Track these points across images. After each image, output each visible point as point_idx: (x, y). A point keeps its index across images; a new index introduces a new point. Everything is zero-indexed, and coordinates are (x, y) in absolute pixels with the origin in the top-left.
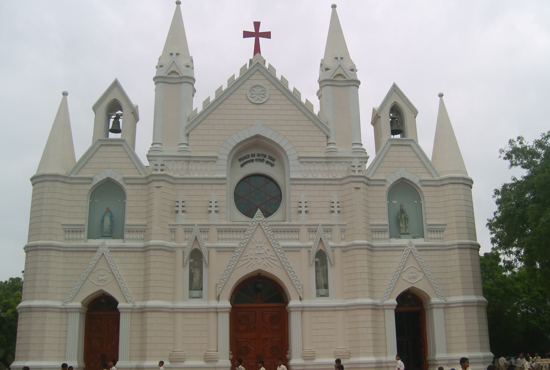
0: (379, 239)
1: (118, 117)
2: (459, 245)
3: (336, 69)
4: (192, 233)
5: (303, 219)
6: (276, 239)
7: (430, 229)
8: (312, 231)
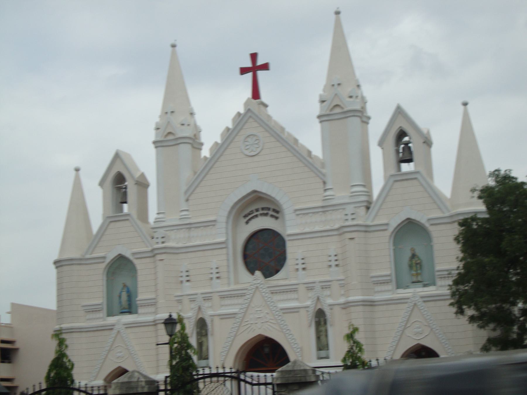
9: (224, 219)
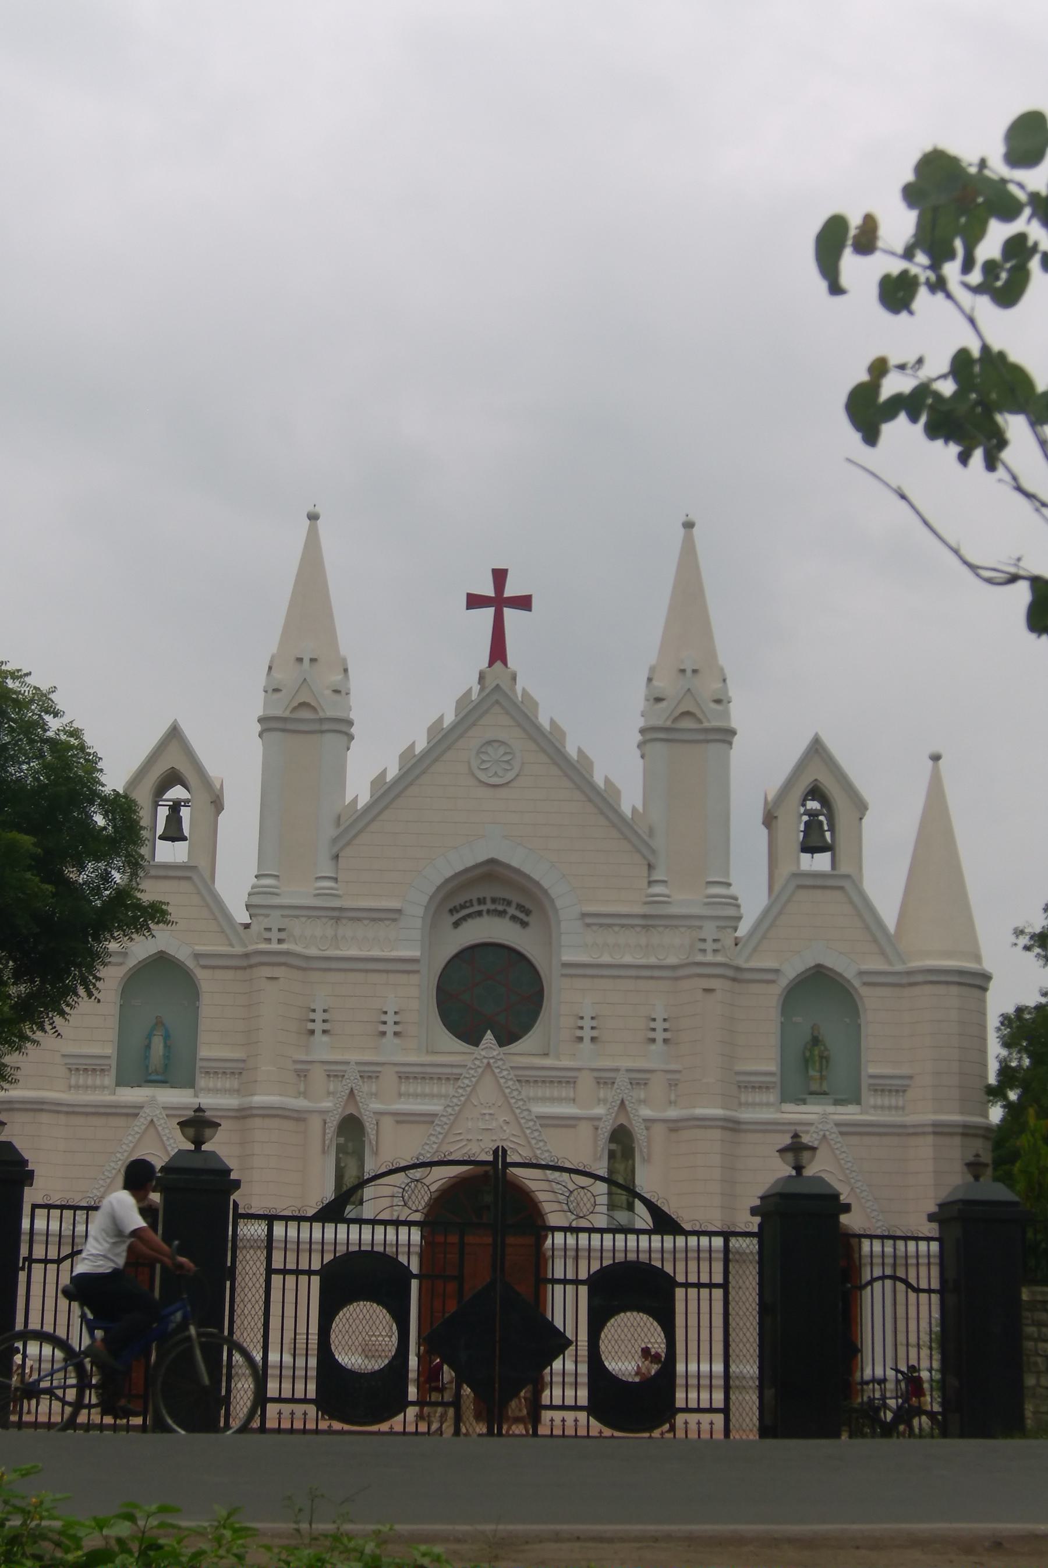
0: (754, 1105)
1: (175, 807)
2: (935, 1125)
4: (344, 1081)
5: (585, 1057)
6: (525, 1099)
7: (875, 1085)
9: (420, 912)
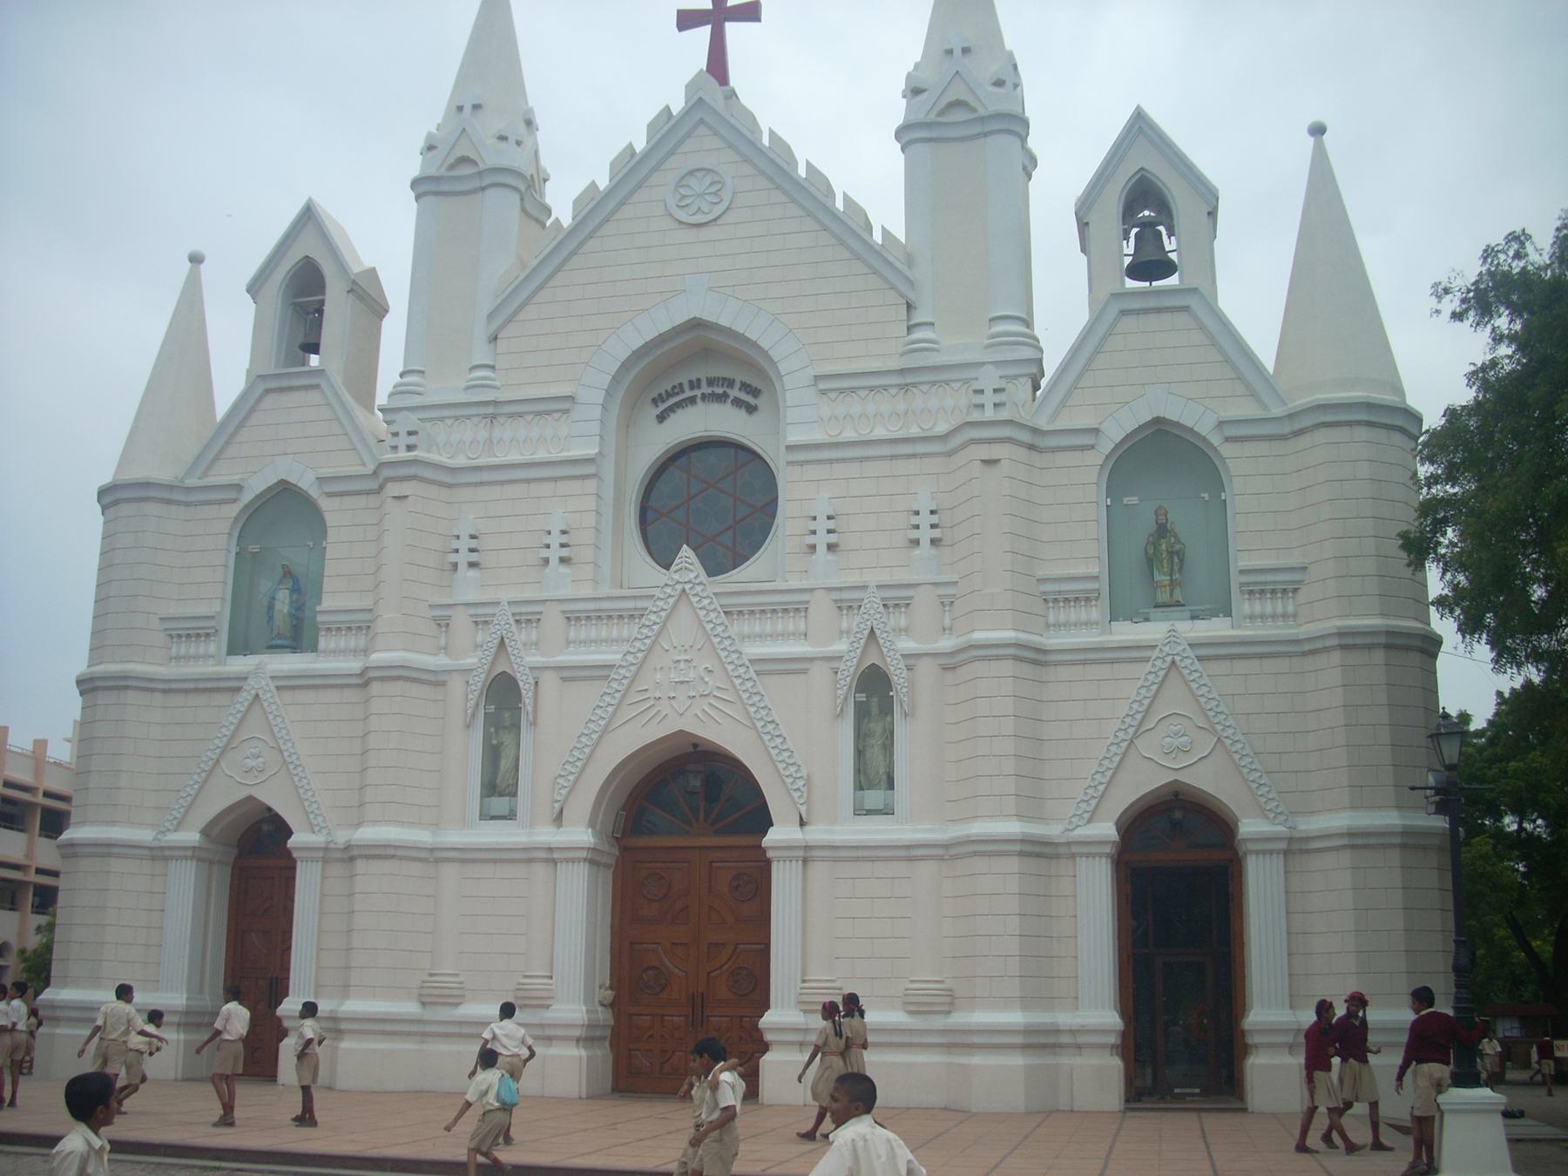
0: (1067, 625)
2: (1341, 634)
3: (946, 88)
5: (824, 571)
7: (1249, 584)
8: (850, 607)
9: (599, 397)
